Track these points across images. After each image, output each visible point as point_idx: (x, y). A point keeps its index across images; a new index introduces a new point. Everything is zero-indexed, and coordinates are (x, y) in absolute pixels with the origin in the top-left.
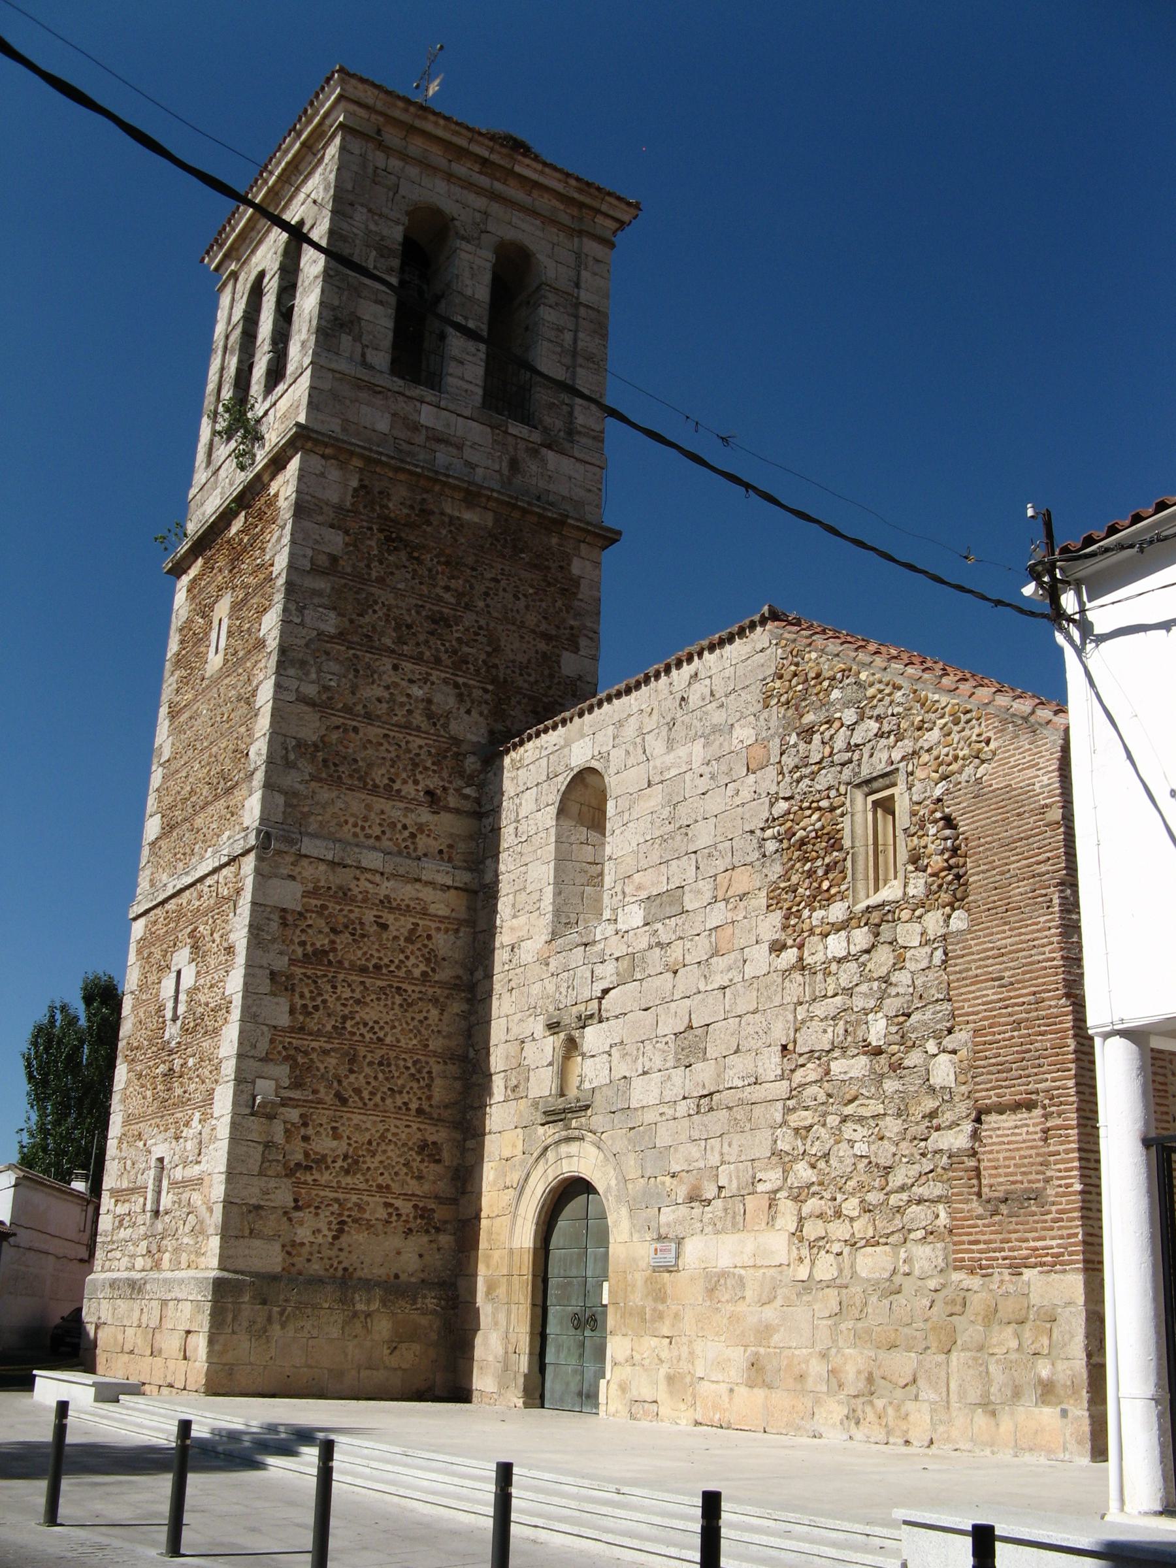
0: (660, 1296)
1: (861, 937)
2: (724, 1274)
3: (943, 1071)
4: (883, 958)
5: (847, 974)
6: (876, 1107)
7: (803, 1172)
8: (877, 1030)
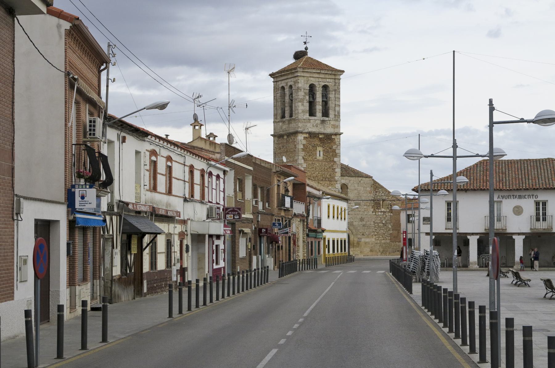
0: (359, 244)
1: (382, 213)
2: (367, 242)
3: (390, 226)
4: (385, 216)
5: (381, 216)
6: (383, 228)
7: (376, 233)
8: (384, 222)
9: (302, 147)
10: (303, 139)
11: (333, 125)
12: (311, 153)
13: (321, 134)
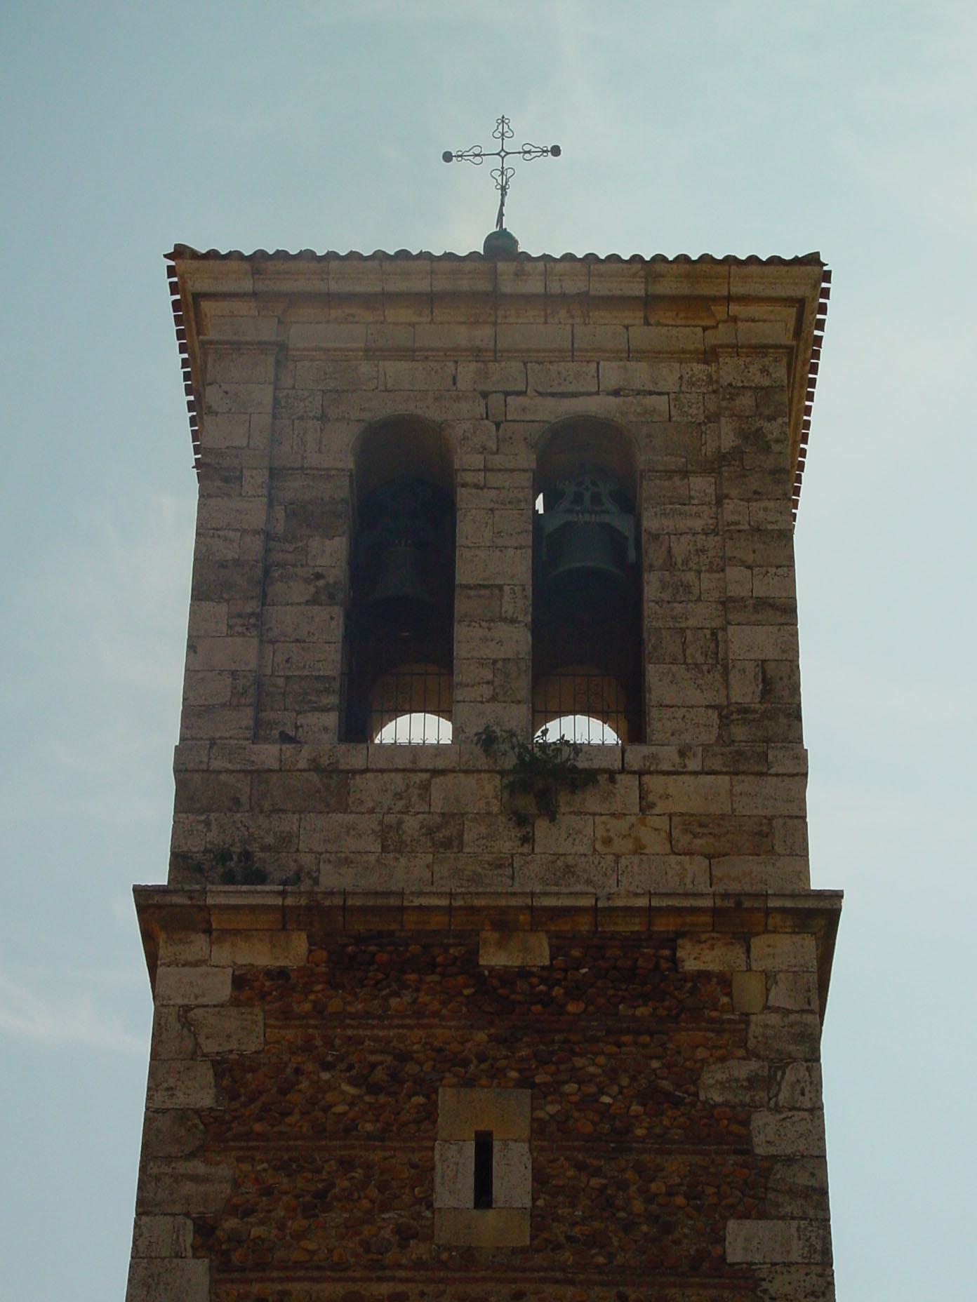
9: (205, 1099)
10: (224, 991)
11: (694, 823)
12: (347, 1165)
13: (504, 923)
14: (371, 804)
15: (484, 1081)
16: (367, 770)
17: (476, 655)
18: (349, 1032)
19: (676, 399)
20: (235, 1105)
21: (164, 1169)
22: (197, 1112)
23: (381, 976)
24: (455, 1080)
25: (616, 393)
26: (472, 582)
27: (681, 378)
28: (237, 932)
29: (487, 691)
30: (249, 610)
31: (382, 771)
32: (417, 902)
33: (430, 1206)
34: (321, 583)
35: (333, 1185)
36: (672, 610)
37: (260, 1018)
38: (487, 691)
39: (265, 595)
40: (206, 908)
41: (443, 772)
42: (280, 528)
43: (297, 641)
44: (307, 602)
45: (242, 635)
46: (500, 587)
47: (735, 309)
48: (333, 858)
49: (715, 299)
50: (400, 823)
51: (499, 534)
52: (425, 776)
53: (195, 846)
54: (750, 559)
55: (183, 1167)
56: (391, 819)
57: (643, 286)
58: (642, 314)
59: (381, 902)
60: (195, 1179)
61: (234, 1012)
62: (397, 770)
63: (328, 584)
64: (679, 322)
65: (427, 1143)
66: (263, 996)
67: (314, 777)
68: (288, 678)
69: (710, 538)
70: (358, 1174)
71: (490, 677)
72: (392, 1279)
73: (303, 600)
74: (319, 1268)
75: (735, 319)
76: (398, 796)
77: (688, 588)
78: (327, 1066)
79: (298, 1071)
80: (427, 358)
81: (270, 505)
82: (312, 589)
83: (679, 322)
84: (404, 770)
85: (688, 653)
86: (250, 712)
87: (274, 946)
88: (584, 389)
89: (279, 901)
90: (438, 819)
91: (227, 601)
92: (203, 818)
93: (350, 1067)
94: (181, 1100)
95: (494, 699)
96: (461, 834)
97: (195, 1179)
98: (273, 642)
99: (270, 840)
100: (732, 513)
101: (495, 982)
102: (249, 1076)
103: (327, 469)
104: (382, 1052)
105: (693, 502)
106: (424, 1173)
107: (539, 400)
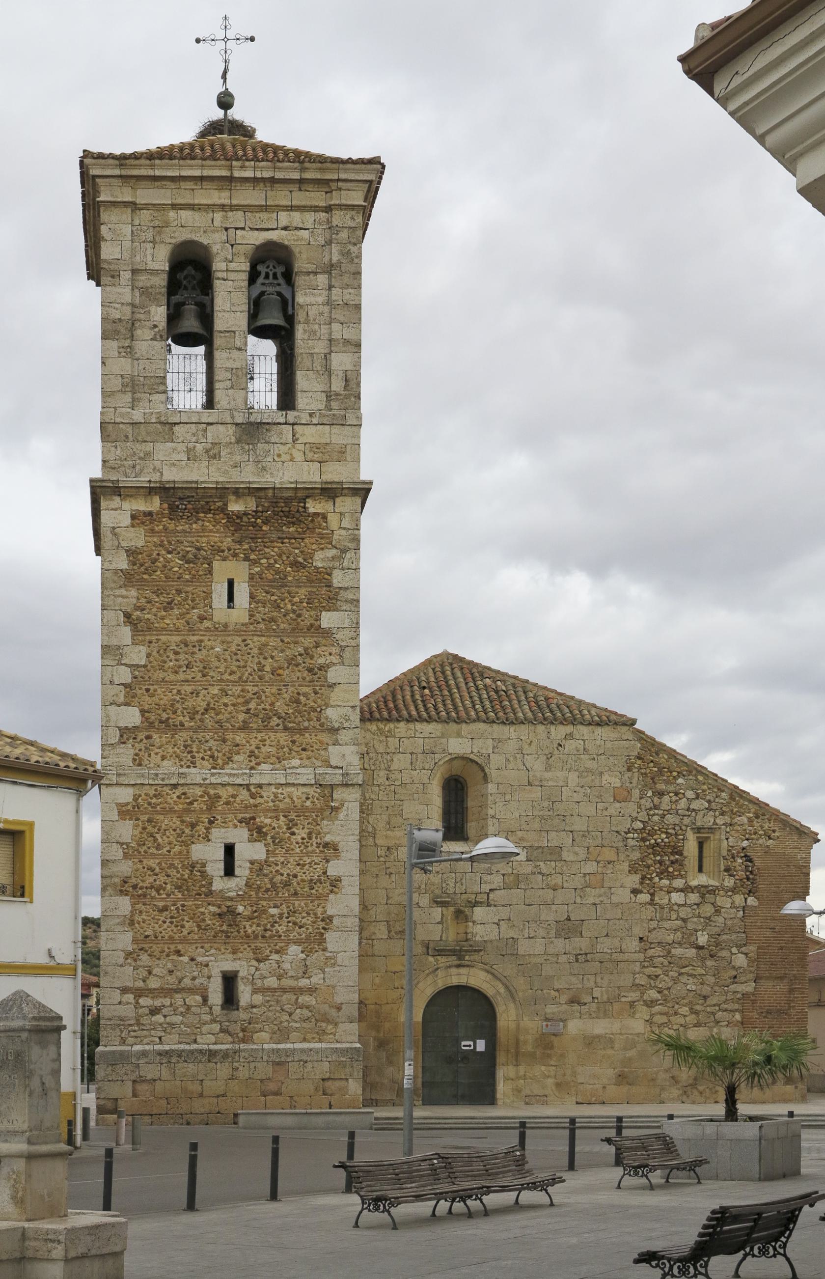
9: (124, 566)
10: (128, 521)
12: (179, 592)
13: (238, 493)
14: (182, 439)
15: (231, 558)
16: (180, 423)
17: (224, 366)
18: (178, 539)
19: (312, 232)
20: (135, 567)
21: (111, 593)
22: (121, 570)
23: (189, 515)
24: (219, 558)
25: (285, 228)
26: (222, 329)
27: (315, 221)
28: (131, 496)
29: (229, 383)
30: (127, 345)
31: (187, 423)
32: (203, 486)
33: (211, 607)
34: (157, 330)
35: (174, 600)
36: (308, 344)
37: (143, 533)
38: (229, 383)
39: (133, 336)
40: (119, 487)
41: (212, 424)
42: (137, 301)
43: (148, 359)
44: (151, 339)
45: (124, 357)
46: (234, 332)
47: (340, 184)
48: (168, 463)
49: (331, 180)
50: (195, 447)
51: (233, 305)
52: (204, 425)
53: (111, 457)
54: (342, 319)
55: (118, 592)
56: (191, 445)
57: (299, 174)
58: (298, 186)
59: (190, 485)
60: (123, 597)
61: (132, 529)
62: (193, 423)
63: (159, 330)
64: (315, 190)
65: (210, 584)
66: (143, 523)
67: (159, 426)
68: (145, 377)
69: (325, 307)
70: (183, 595)
71: (230, 377)
72: (198, 635)
73: (149, 338)
74: (171, 631)
75: (340, 189)
76: (194, 435)
77: (315, 332)
78: (169, 553)
79: (158, 554)
80: (200, 209)
81: (133, 290)
82: (153, 333)
83: (315, 190)
84: (195, 423)
85: (314, 365)
86: (130, 394)
87: (146, 502)
88: (270, 227)
89: (148, 485)
90: (210, 445)
91: (117, 339)
92: (114, 444)
93: (179, 553)
94: (114, 566)
95: (232, 387)
96: (220, 452)
97: (123, 597)
98: (138, 359)
99: (142, 455)
100: (336, 295)
101: (234, 517)
102: (140, 556)
103: (157, 270)
104: (190, 546)
105: (319, 288)
106: (208, 595)
107: (251, 233)
